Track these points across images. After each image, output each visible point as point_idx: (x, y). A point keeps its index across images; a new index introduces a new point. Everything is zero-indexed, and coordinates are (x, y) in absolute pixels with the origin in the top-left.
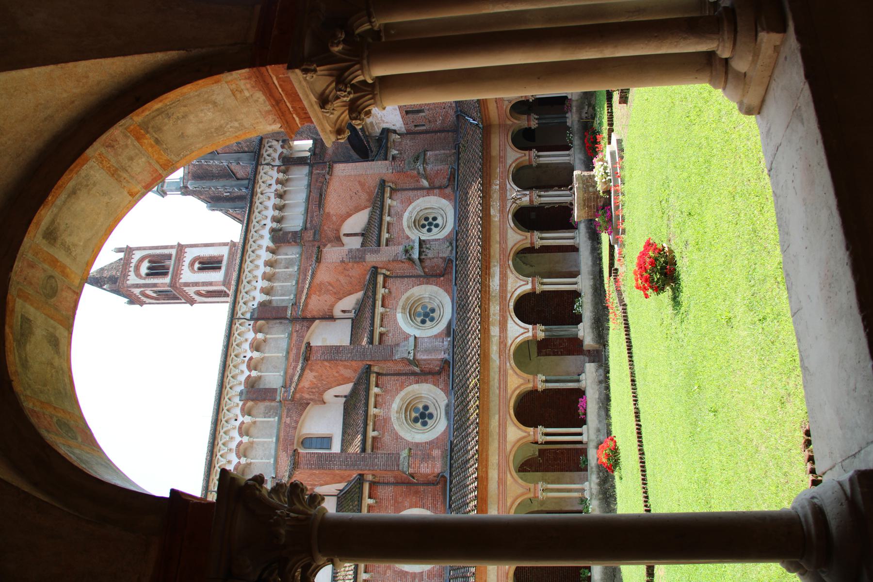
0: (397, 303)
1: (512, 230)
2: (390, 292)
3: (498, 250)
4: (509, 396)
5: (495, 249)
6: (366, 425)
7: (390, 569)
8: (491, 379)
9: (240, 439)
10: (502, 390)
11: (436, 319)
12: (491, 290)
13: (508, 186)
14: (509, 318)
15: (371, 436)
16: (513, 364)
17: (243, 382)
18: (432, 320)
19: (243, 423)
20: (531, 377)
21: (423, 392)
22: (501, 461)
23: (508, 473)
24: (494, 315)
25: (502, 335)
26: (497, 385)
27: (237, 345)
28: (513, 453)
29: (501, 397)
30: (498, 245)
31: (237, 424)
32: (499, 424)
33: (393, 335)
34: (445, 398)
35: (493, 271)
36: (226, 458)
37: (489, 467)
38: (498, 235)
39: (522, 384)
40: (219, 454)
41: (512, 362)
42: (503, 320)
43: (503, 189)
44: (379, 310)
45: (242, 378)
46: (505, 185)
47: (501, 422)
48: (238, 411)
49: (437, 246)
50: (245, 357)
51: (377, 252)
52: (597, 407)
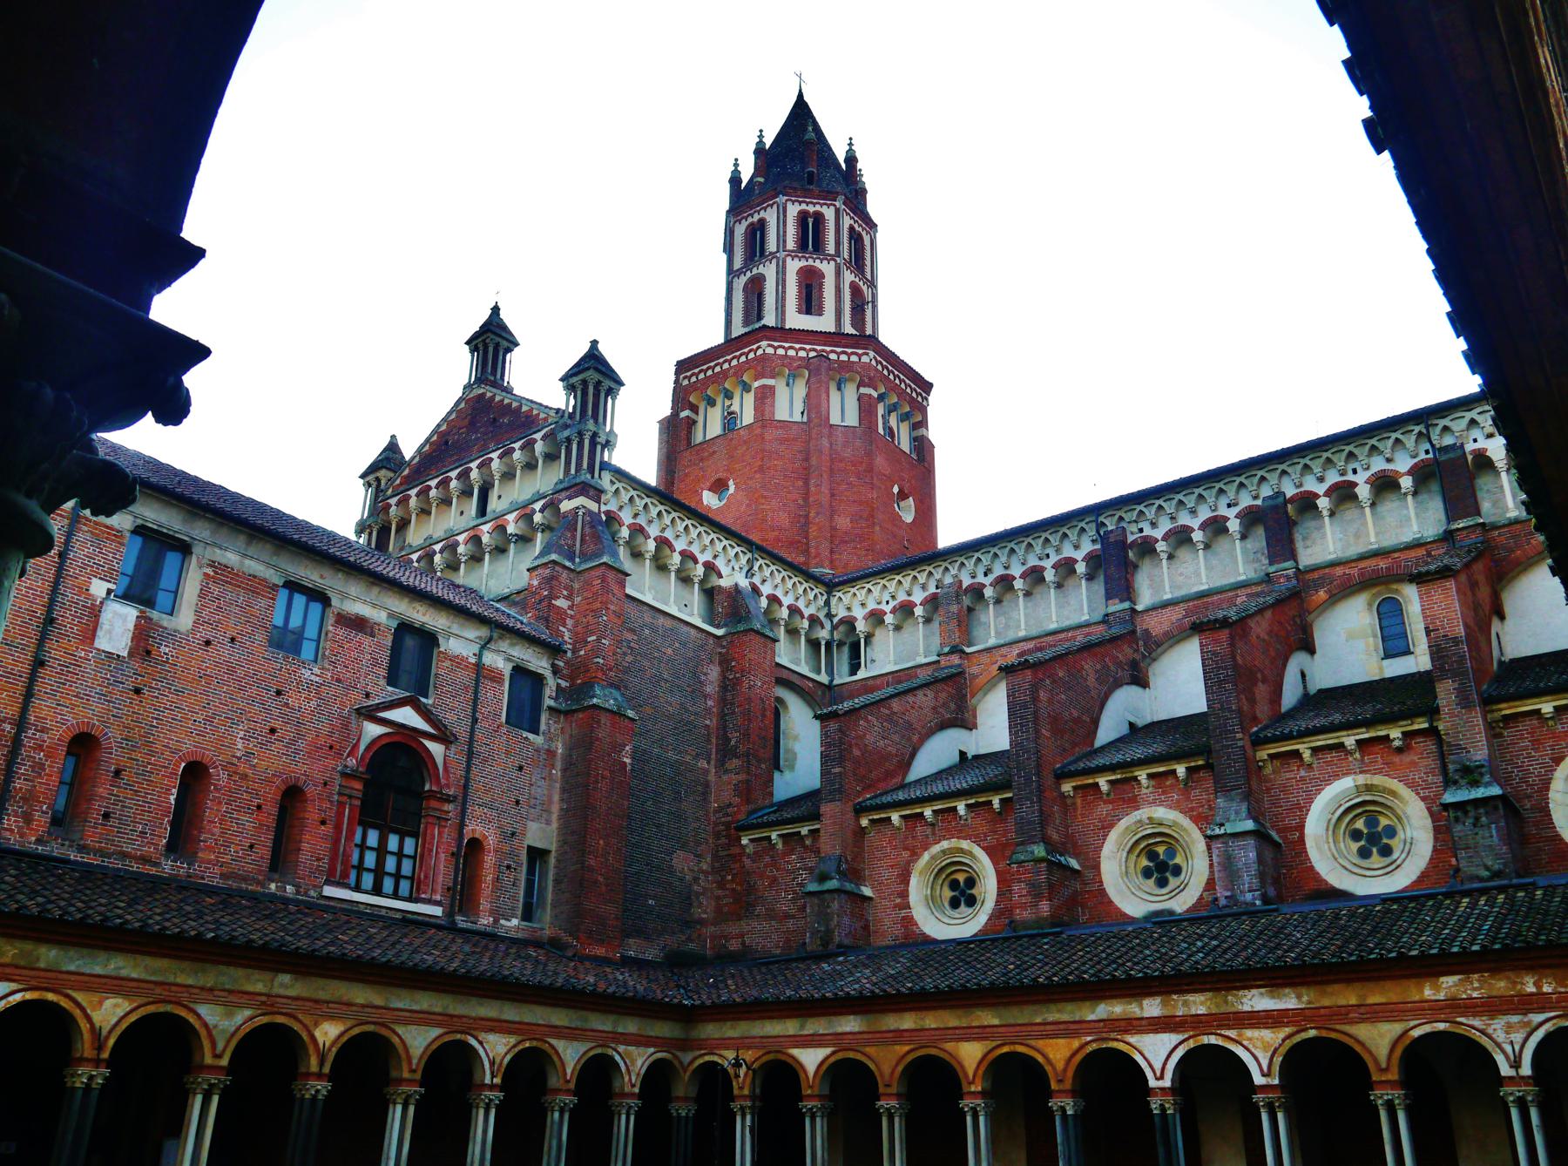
0: (1379, 772)
2: (1399, 750)
3: (1343, 1002)
4: (1033, 1043)
6: (1111, 768)
7: (911, 856)
8: (1060, 1006)
9: (1196, 527)
10: (1042, 1028)
11: (1365, 863)
12: (1241, 993)
13: (1537, 1018)
14: (1181, 1037)
15: (1097, 780)
16: (1089, 1049)
17: (1302, 489)
18: (1364, 853)
19: (1226, 519)
20: (1068, 1085)
21: (1195, 861)
22: (927, 1033)
23: (912, 1046)
24: (1186, 1003)
25: (1144, 1022)
26: (1051, 1017)
27: (1374, 448)
28: (942, 1055)
29: (1029, 1029)
30: (1353, 1001)
31: (1223, 511)
32: (985, 1027)
34: (1185, 907)
35: (1285, 995)
37: (919, 1013)
38: (1384, 1000)
40: (1160, 502)
41: (1095, 1046)
42: (1176, 1023)
43: (1526, 1004)
44: (1350, 741)
45: (1311, 485)
46: (1542, 1010)
47: (988, 1030)
48: (1246, 501)
49: (1488, 842)
50: (1355, 471)
51: (1464, 702)
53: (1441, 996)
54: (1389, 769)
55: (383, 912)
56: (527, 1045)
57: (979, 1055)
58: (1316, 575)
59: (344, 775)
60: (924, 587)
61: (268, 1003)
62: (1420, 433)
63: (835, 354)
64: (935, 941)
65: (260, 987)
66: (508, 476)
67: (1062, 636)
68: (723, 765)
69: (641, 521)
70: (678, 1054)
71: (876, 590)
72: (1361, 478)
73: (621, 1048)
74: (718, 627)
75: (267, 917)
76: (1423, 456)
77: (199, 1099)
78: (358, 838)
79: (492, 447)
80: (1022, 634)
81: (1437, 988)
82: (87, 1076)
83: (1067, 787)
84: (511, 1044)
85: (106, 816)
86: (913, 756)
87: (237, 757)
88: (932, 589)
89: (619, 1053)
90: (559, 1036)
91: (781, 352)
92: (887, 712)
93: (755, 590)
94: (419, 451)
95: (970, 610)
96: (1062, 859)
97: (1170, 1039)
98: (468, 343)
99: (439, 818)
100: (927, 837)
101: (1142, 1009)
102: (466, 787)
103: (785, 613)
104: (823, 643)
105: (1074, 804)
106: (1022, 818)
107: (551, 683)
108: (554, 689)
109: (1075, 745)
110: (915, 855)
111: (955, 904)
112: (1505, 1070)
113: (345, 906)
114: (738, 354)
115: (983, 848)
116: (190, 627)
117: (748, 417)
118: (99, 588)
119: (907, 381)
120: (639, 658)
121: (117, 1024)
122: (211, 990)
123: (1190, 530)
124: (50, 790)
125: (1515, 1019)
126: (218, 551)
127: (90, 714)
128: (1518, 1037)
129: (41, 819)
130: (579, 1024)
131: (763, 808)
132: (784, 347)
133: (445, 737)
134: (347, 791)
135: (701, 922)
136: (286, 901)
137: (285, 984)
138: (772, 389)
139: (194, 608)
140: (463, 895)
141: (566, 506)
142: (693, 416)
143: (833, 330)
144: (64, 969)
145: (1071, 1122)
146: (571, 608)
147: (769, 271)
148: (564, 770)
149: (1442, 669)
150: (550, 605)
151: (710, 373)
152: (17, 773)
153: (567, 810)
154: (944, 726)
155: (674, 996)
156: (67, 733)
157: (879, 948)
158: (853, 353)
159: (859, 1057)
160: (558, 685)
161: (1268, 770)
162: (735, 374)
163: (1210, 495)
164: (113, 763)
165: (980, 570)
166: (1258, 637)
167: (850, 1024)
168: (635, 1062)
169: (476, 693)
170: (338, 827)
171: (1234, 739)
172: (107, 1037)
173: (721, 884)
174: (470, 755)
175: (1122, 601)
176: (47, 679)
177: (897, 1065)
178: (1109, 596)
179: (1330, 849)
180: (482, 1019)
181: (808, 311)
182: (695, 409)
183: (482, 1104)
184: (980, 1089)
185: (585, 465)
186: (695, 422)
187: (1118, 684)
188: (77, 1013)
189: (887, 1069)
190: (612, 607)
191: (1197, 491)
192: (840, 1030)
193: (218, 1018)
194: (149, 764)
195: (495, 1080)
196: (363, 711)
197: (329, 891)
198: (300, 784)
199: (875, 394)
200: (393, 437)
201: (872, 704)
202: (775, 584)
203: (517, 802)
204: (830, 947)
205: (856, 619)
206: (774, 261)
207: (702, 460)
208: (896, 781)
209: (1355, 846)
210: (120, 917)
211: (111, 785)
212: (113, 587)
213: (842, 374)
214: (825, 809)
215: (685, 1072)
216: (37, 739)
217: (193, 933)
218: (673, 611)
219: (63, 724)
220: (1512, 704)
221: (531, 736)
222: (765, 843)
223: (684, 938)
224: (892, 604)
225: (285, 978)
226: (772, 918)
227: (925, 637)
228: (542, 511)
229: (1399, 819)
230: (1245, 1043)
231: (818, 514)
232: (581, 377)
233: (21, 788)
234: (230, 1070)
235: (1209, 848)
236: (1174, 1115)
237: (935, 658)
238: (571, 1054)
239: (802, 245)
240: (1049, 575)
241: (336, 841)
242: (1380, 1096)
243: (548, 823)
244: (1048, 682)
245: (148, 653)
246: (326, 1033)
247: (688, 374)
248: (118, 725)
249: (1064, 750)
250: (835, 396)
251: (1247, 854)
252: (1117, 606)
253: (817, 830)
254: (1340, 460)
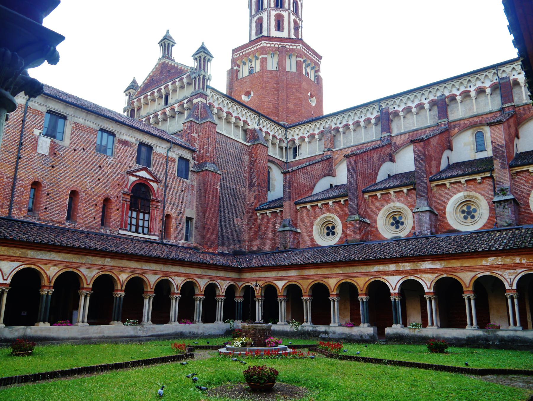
0: (472, 191)
1: (474, 275)
2: (480, 183)
4: (353, 279)
5: (456, 264)
6: (382, 189)
8: (362, 267)
10: (356, 274)
12: (422, 263)
13: (521, 271)
14: (402, 277)
16: (372, 280)
17: (451, 93)
18: (465, 218)
19: (424, 104)
20: (364, 292)
21: (409, 220)
24: (403, 266)
25: (390, 272)
26: (359, 271)
27: (477, 78)
28: (323, 282)
29: (352, 274)
30: (459, 266)
31: (423, 101)
32: (337, 274)
33: (446, 193)
34: (405, 236)
36: (407, 101)
37: (316, 270)
39: (360, 287)
40: (401, 98)
41: (373, 280)
43: (516, 266)
44: (463, 180)
45: (455, 92)
46: (521, 268)
47: (338, 275)
48: (431, 97)
49: (507, 214)
51: (503, 167)
52: (347, 333)
53: (488, 264)
54: (476, 190)
55: (139, 239)
56: (188, 280)
57: (335, 283)
58: (454, 123)
59: (124, 194)
60: (319, 128)
61: (103, 267)
62: (494, 73)
63: (288, 45)
64: (322, 247)
65: (100, 263)
66: (175, 91)
67: (366, 145)
69: (221, 106)
70: (237, 283)
71: (302, 130)
72: (472, 89)
73: (219, 281)
74: (248, 142)
75: (101, 240)
76: (495, 81)
77: (83, 298)
78: (129, 215)
79: (169, 80)
80: (352, 144)
81: (487, 261)
82: (47, 291)
83: (366, 196)
85: (46, 208)
86: (314, 186)
88: (322, 129)
89: (218, 283)
90: (198, 278)
91: (269, 45)
92: (306, 171)
93: (261, 130)
94: (143, 83)
95: (334, 136)
96: (364, 220)
97: (398, 278)
98: (159, 43)
99: (156, 208)
100: (319, 212)
101: (389, 268)
102: (164, 197)
103: (271, 138)
104: (284, 148)
105: (369, 201)
106: (351, 206)
107: (192, 163)
109: (369, 182)
110: (315, 219)
111: (328, 234)
112: (507, 287)
113: (127, 237)
114: (254, 46)
115: (338, 216)
116: (69, 145)
117: (257, 69)
118: (37, 132)
119: (314, 55)
120: (221, 153)
121: (55, 275)
122: (84, 264)
123: (410, 108)
125: (512, 271)
126: (76, 118)
127: (37, 176)
128: (512, 277)
129: (25, 210)
131: (263, 204)
132: (270, 43)
133: (157, 181)
134: (125, 199)
135: (244, 241)
136: (107, 235)
137: (108, 262)
138: (266, 58)
139: (70, 138)
140: (165, 232)
141: (195, 101)
142: (238, 69)
143: (287, 37)
144: (36, 258)
145: (365, 303)
146: (198, 136)
147: (264, 15)
148: (197, 191)
149: (496, 156)
150: (191, 136)
151: (244, 53)
153: (199, 205)
154: (325, 176)
155: (236, 265)
157: (303, 249)
158: (294, 45)
159: (296, 283)
160: (194, 163)
161: (435, 190)
162: (253, 53)
163: (419, 95)
165: (338, 122)
166: (433, 145)
167: (293, 273)
168: (223, 286)
169: (167, 166)
170: (123, 211)
171: (424, 180)
172: (52, 279)
173: (251, 229)
174: (166, 187)
175: (387, 133)
176: (22, 163)
177: (309, 285)
178: (383, 131)
179: (454, 216)
180: (173, 272)
181: (279, 30)
182: (239, 66)
183: (174, 299)
184: (335, 293)
185: (201, 87)
186: (239, 71)
187: (384, 161)
188: (42, 272)
189: (305, 287)
190: (212, 136)
191: (415, 94)
192: (290, 275)
195: (178, 291)
197: (121, 232)
198: (109, 197)
199: (302, 60)
200: (134, 78)
201: (301, 168)
202: (267, 127)
203: (182, 202)
204: (287, 248)
205: (295, 139)
206: (266, 12)
207: (242, 84)
208: (309, 194)
209: (463, 215)
210: (53, 241)
212: (41, 131)
213: (290, 53)
214: (285, 204)
215: (239, 288)
217: (77, 246)
218: (233, 137)
220: (519, 168)
221: (186, 180)
222: (265, 215)
223: (238, 246)
224: (308, 134)
225: (108, 260)
226: (267, 239)
227: (319, 146)
228: (187, 103)
229: (478, 206)
230: (422, 279)
231: (282, 103)
232: (199, 55)
234: (93, 289)
235: (413, 216)
236: (398, 301)
237: (322, 153)
238: (202, 283)
239: (277, 6)
240: (362, 124)
241: (122, 216)
242: (465, 296)
243: (192, 209)
244: (361, 160)
245: (55, 154)
247: (236, 53)
249: (366, 183)
250: (288, 61)
251: (426, 218)
252: (385, 134)
253: (282, 211)
254: (465, 83)
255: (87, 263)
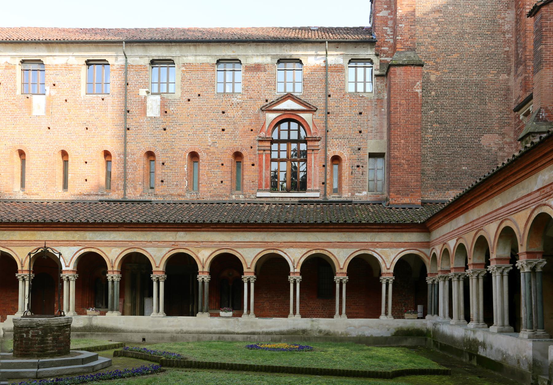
65: (171, 239)
68: (516, 73)
84: (304, 253)
87: (209, 145)
90: (334, 247)
108: (379, 64)
121: (117, 258)
122: (150, 242)
124: (141, 176)
130: (347, 240)
133: (311, 109)
137: (182, 236)
144: (96, 240)
152: (128, 172)
156: (142, 153)
164: (160, 161)
193: (156, 252)
194: (174, 157)
196: (263, 109)
211: (161, 169)
216: (132, 158)
219: (140, 150)
225: (181, 234)
233: (131, 178)
246: (204, 255)
248: (160, 145)
255: (154, 240)
